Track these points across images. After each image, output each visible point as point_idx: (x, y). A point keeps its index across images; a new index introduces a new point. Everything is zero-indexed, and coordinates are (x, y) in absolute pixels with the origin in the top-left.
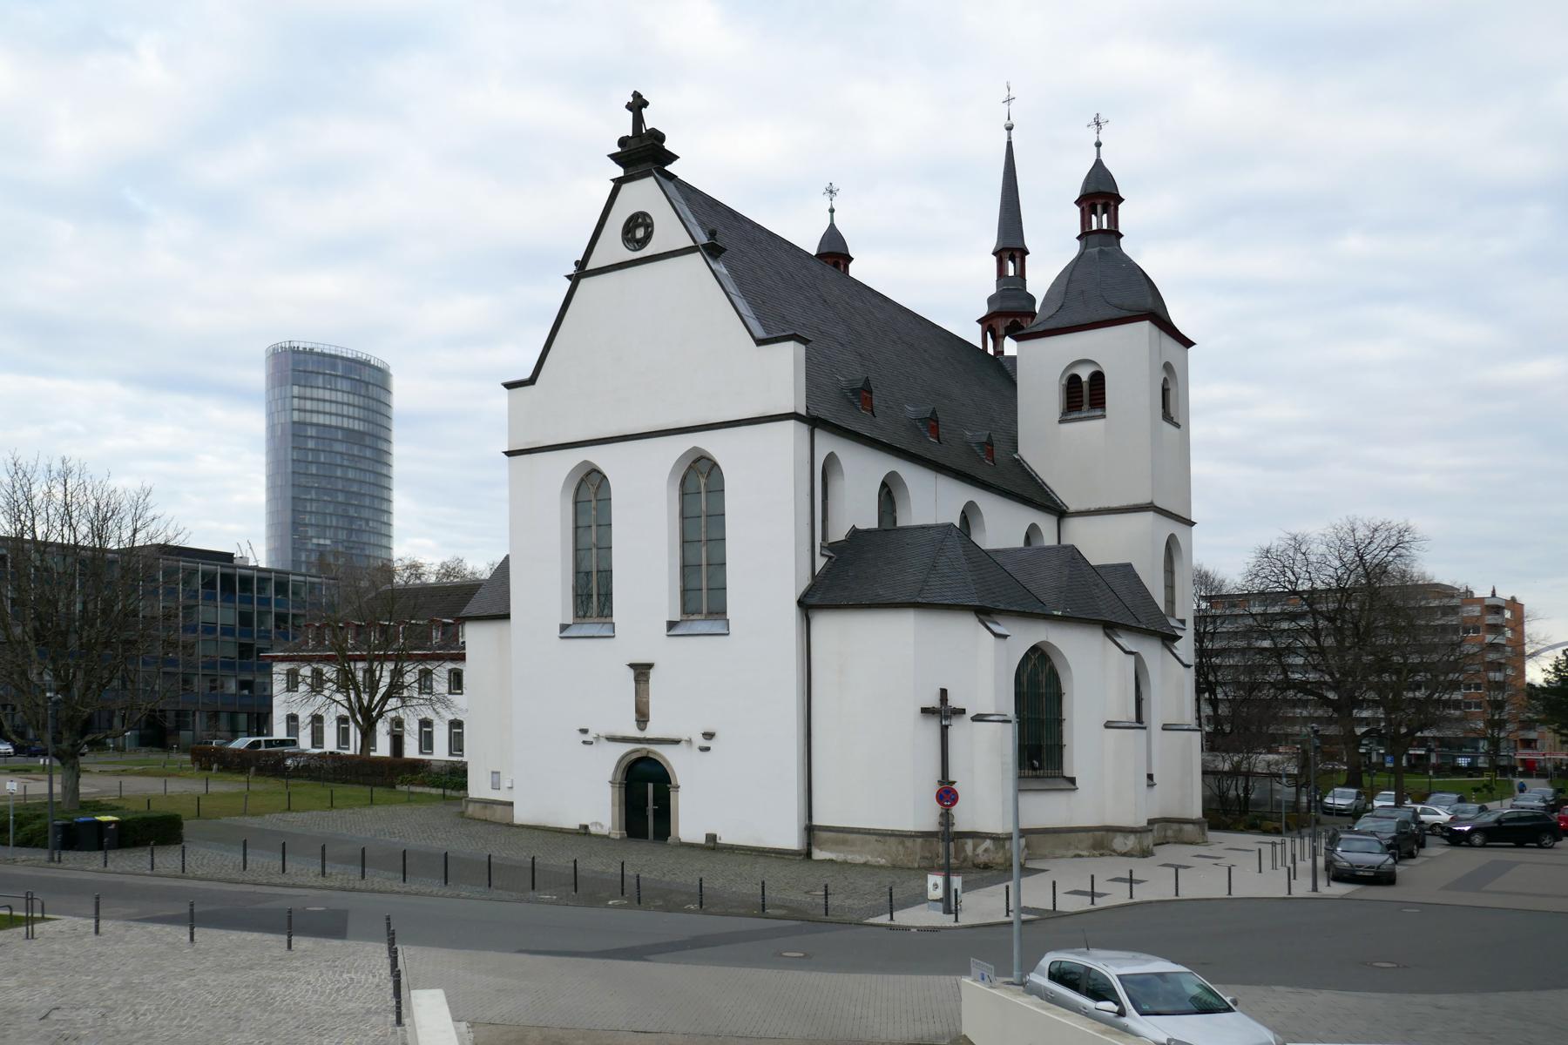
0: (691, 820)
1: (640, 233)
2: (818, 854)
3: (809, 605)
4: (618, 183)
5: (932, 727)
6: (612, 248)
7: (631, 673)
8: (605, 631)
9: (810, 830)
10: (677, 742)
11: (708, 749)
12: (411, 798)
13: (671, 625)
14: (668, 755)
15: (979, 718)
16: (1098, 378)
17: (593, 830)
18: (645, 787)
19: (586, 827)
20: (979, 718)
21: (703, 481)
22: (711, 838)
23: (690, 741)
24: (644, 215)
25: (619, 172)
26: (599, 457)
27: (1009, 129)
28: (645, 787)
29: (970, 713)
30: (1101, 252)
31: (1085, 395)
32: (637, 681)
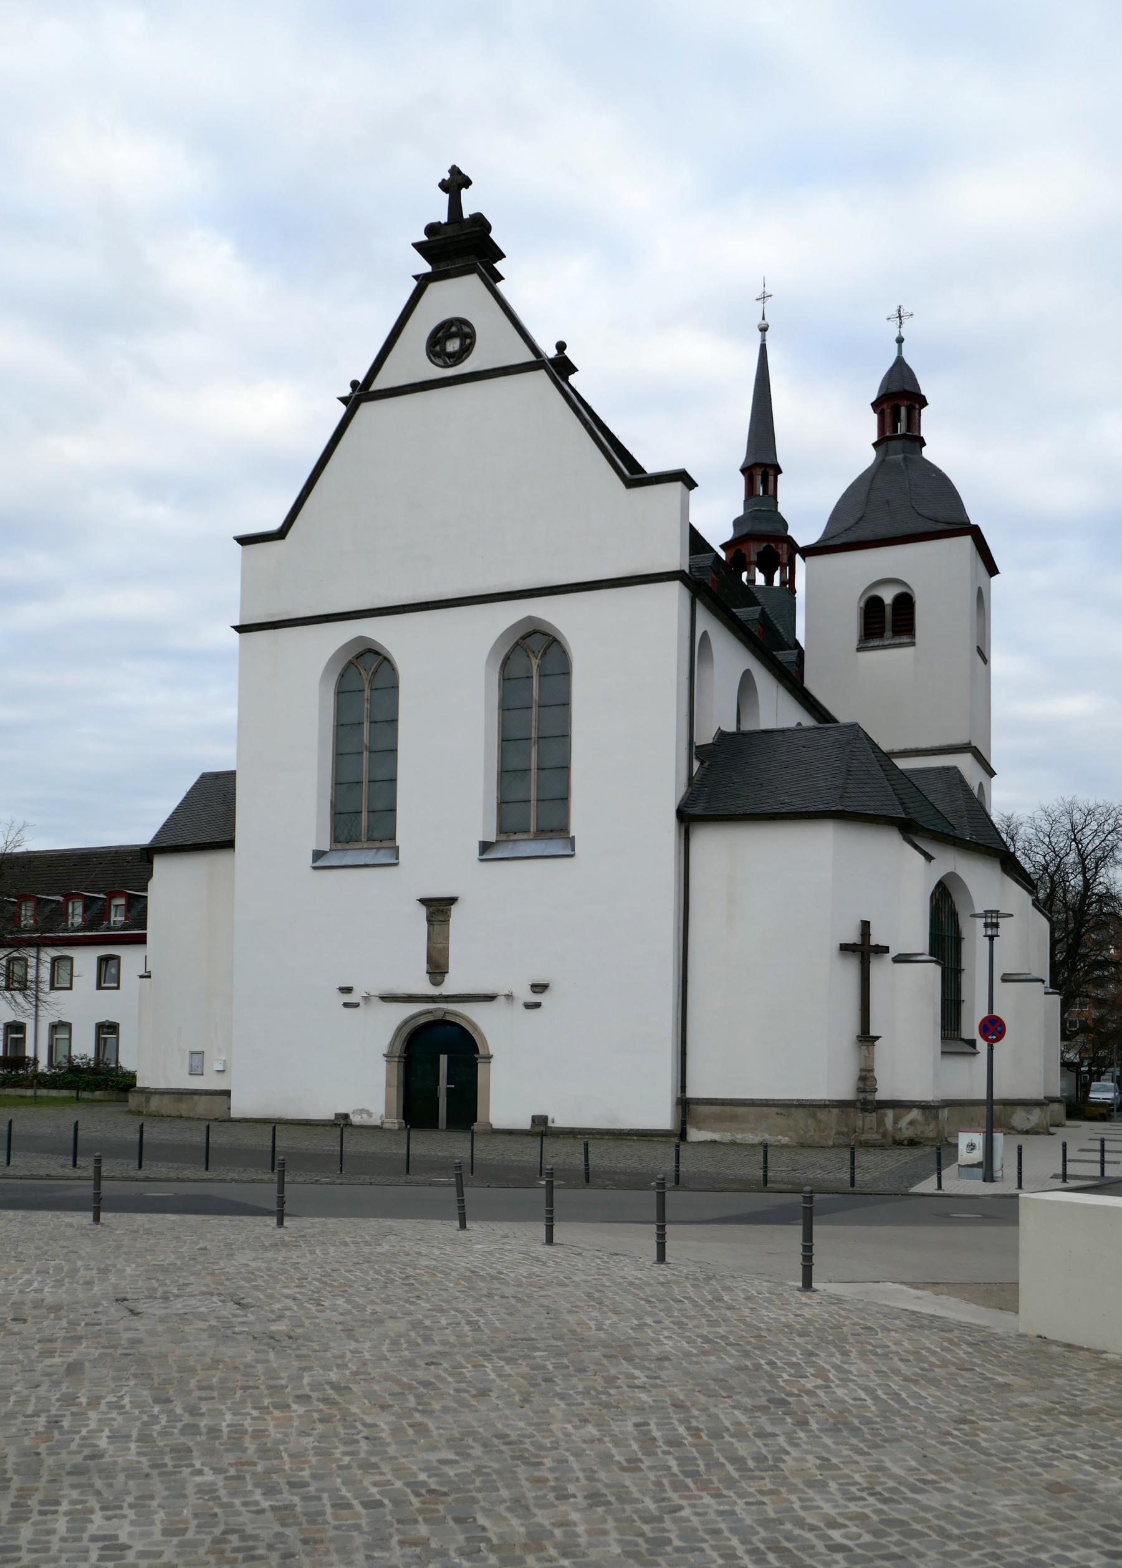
0: (509, 1097)
1: (453, 346)
2: (695, 1135)
3: (689, 817)
4: (423, 282)
5: (850, 968)
6: (412, 362)
7: (423, 911)
8: (383, 857)
9: (685, 1105)
10: (490, 998)
11: (537, 1005)
12: (36, 1100)
13: (485, 847)
14: (476, 1015)
15: (902, 959)
17: (356, 1119)
18: (438, 1060)
19: (346, 1116)
20: (902, 959)
21: (535, 662)
22: (540, 1121)
23: (509, 997)
24: (463, 322)
25: (426, 268)
26: (382, 632)
27: (764, 330)
28: (438, 1060)
29: (893, 953)
30: (905, 459)
32: (430, 921)
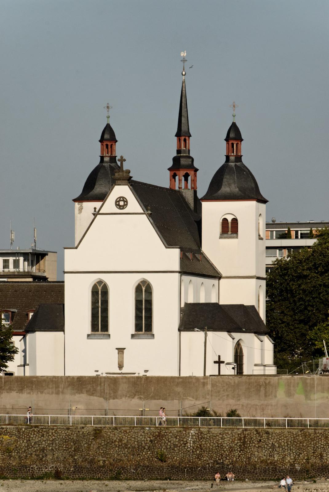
7: (117, 351)
15: (228, 364)
16: (235, 221)
20: (228, 364)
29: (225, 363)
31: (230, 228)
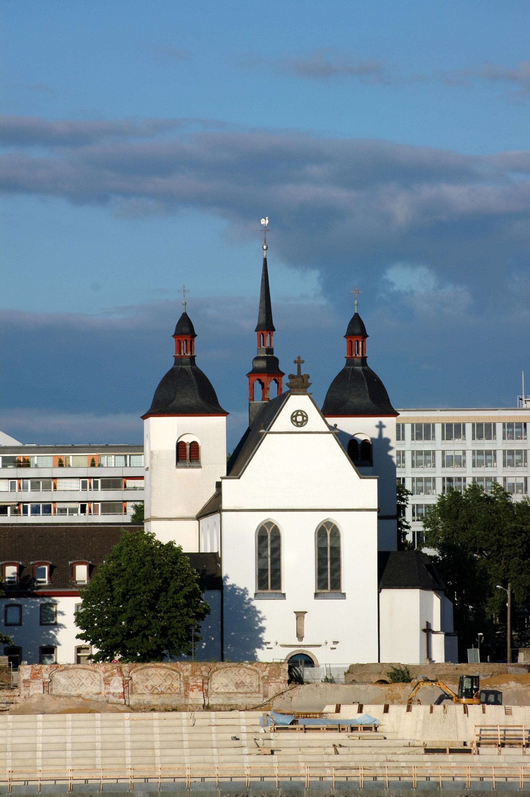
1: (300, 419)
7: (295, 615)
11: (335, 648)
14: (313, 652)
